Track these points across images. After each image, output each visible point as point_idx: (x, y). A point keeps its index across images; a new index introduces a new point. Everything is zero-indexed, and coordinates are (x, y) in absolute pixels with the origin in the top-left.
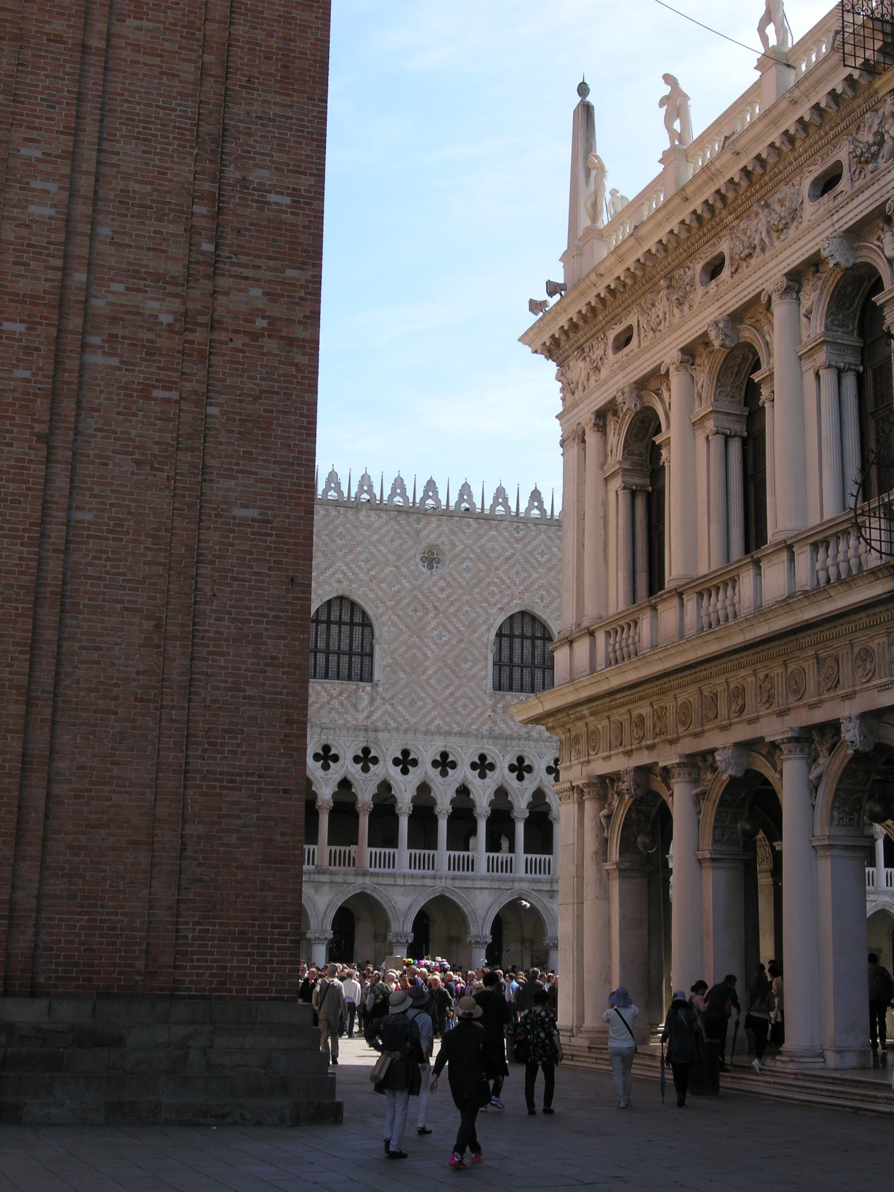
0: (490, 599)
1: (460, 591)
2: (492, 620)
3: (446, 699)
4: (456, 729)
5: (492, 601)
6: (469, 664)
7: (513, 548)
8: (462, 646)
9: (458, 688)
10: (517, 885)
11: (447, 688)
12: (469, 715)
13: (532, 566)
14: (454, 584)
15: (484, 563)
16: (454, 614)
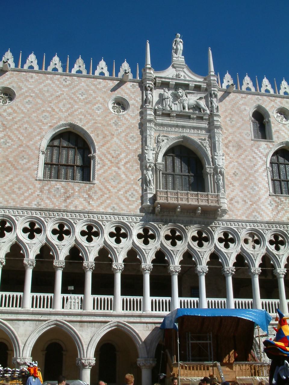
0: (43, 120)
1: (23, 115)
2: (44, 133)
3: (6, 184)
4: (12, 204)
5: (45, 121)
6: (25, 161)
7: (62, 91)
8: (22, 149)
9: (17, 176)
10: (53, 318)
11: (7, 176)
12: (23, 194)
13: (75, 101)
14: (18, 111)
15: (41, 99)
16: (17, 129)
